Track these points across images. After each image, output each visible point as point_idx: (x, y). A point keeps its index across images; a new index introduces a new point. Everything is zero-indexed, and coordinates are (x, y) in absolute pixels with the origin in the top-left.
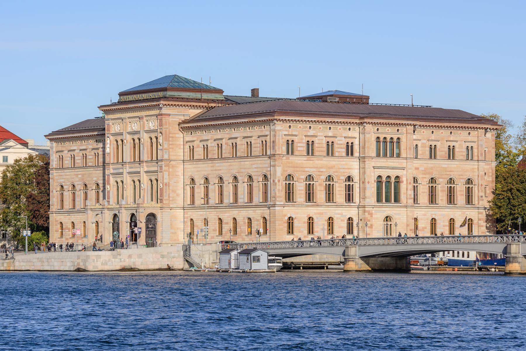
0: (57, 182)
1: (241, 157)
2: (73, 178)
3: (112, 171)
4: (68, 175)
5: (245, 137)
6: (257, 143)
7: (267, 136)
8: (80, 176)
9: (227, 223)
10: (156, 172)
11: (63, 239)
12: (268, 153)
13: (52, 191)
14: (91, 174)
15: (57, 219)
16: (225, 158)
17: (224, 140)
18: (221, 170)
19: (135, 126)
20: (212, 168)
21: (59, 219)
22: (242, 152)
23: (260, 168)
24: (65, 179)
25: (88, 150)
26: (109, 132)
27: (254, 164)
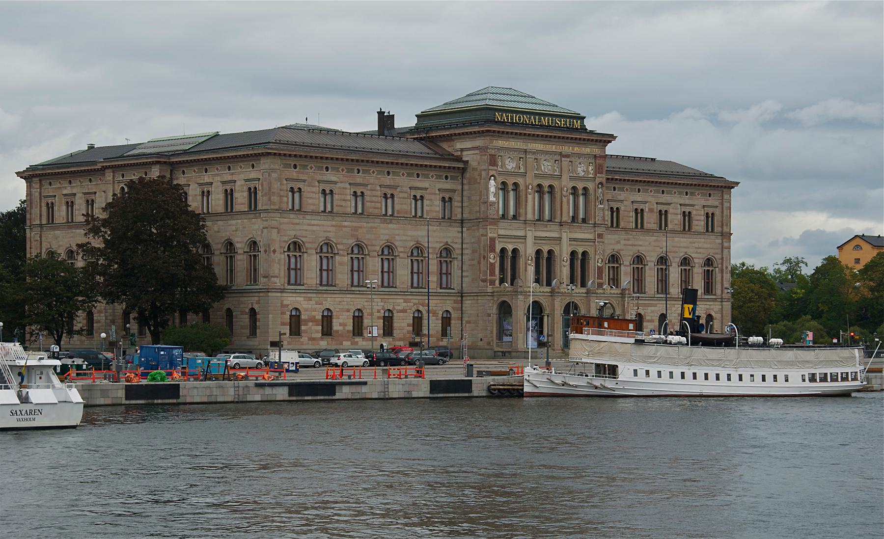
0: (285, 236)
1: (674, 232)
2: (330, 232)
3: (501, 232)
4: (313, 225)
5: (681, 205)
6: (701, 215)
7: (717, 207)
8: (344, 229)
9: (652, 321)
10: (594, 241)
11: (301, 340)
12: (717, 229)
13: (274, 251)
14: (376, 228)
15: (285, 302)
16: (649, 231)
17: (647, 205)
18: (641, 246)
19: (547, 166)
20: (627, 242)
21: (289, 303)
22: (676, 224)
23: (703, 248)
24: (306, 230)
25: (369, 187)
26: (495, 168)
27: (694, 243)
